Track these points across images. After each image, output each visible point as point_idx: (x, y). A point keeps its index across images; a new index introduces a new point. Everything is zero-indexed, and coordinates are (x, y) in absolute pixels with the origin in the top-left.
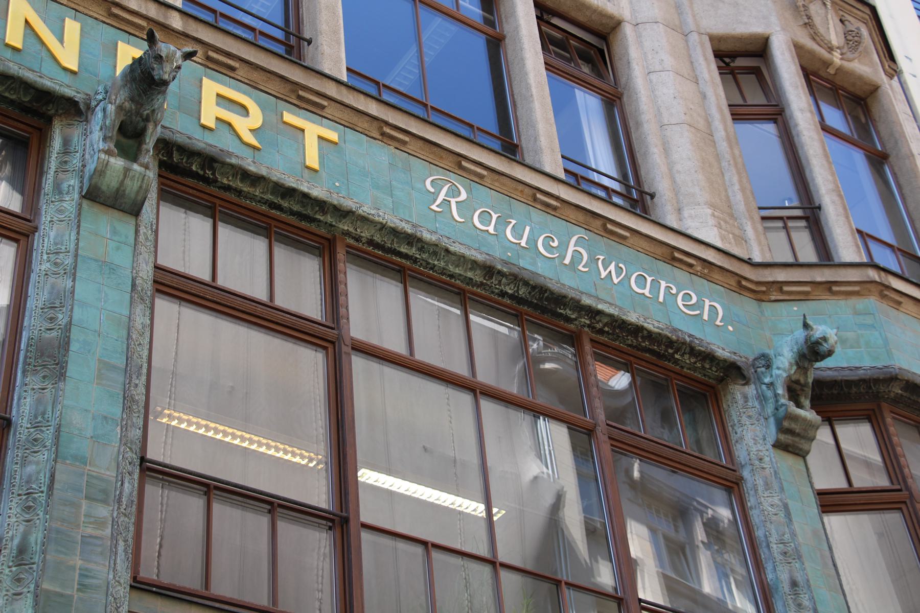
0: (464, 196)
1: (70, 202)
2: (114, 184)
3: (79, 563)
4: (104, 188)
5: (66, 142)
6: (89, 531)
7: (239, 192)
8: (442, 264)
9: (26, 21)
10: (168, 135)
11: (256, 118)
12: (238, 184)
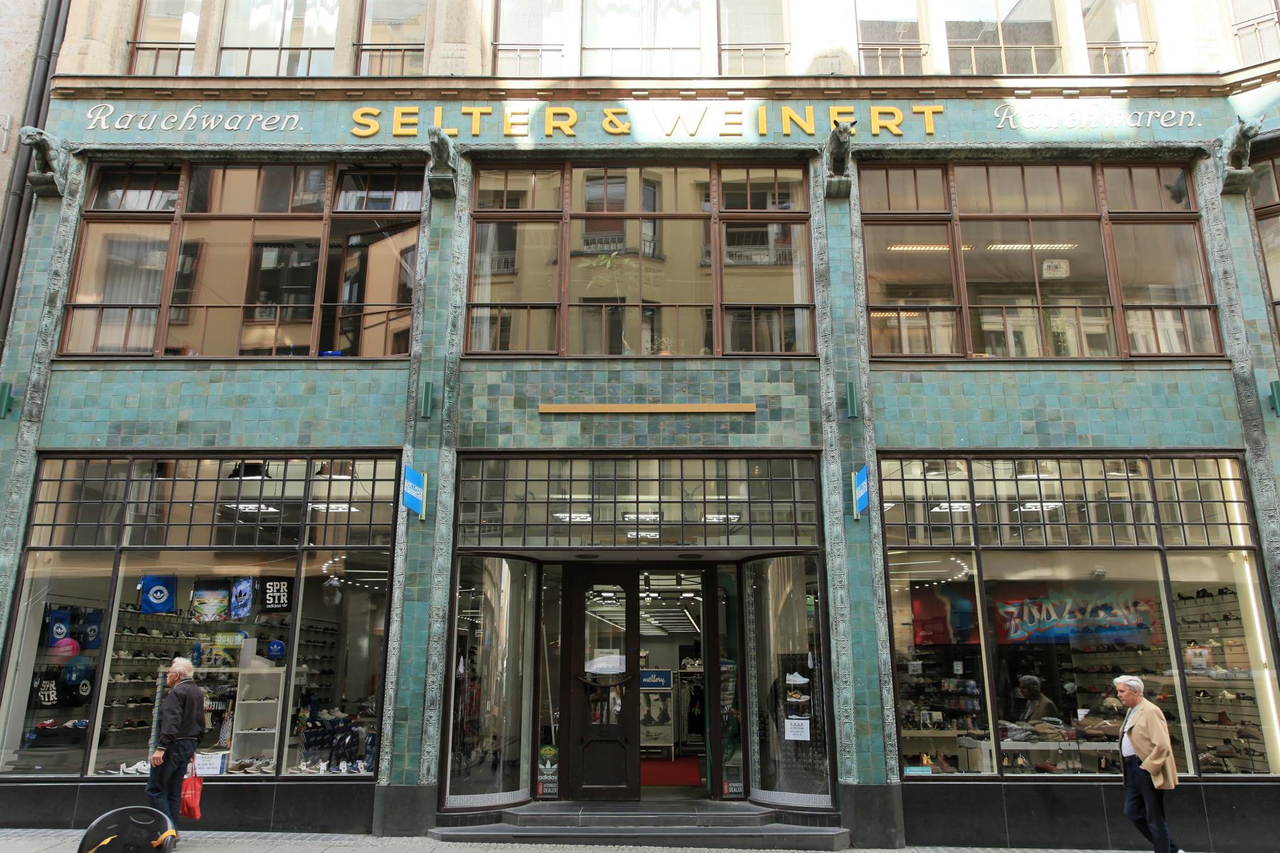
1: (821, 203)
2: (836, 189)
3: (847, 359)
4: (832, 192)
5: (815, 172)
6: (849, 346)
7: (897, 159)
8: (1007, 156)
9: (791, 118)
10: (857, 148)
12: (895, 156)
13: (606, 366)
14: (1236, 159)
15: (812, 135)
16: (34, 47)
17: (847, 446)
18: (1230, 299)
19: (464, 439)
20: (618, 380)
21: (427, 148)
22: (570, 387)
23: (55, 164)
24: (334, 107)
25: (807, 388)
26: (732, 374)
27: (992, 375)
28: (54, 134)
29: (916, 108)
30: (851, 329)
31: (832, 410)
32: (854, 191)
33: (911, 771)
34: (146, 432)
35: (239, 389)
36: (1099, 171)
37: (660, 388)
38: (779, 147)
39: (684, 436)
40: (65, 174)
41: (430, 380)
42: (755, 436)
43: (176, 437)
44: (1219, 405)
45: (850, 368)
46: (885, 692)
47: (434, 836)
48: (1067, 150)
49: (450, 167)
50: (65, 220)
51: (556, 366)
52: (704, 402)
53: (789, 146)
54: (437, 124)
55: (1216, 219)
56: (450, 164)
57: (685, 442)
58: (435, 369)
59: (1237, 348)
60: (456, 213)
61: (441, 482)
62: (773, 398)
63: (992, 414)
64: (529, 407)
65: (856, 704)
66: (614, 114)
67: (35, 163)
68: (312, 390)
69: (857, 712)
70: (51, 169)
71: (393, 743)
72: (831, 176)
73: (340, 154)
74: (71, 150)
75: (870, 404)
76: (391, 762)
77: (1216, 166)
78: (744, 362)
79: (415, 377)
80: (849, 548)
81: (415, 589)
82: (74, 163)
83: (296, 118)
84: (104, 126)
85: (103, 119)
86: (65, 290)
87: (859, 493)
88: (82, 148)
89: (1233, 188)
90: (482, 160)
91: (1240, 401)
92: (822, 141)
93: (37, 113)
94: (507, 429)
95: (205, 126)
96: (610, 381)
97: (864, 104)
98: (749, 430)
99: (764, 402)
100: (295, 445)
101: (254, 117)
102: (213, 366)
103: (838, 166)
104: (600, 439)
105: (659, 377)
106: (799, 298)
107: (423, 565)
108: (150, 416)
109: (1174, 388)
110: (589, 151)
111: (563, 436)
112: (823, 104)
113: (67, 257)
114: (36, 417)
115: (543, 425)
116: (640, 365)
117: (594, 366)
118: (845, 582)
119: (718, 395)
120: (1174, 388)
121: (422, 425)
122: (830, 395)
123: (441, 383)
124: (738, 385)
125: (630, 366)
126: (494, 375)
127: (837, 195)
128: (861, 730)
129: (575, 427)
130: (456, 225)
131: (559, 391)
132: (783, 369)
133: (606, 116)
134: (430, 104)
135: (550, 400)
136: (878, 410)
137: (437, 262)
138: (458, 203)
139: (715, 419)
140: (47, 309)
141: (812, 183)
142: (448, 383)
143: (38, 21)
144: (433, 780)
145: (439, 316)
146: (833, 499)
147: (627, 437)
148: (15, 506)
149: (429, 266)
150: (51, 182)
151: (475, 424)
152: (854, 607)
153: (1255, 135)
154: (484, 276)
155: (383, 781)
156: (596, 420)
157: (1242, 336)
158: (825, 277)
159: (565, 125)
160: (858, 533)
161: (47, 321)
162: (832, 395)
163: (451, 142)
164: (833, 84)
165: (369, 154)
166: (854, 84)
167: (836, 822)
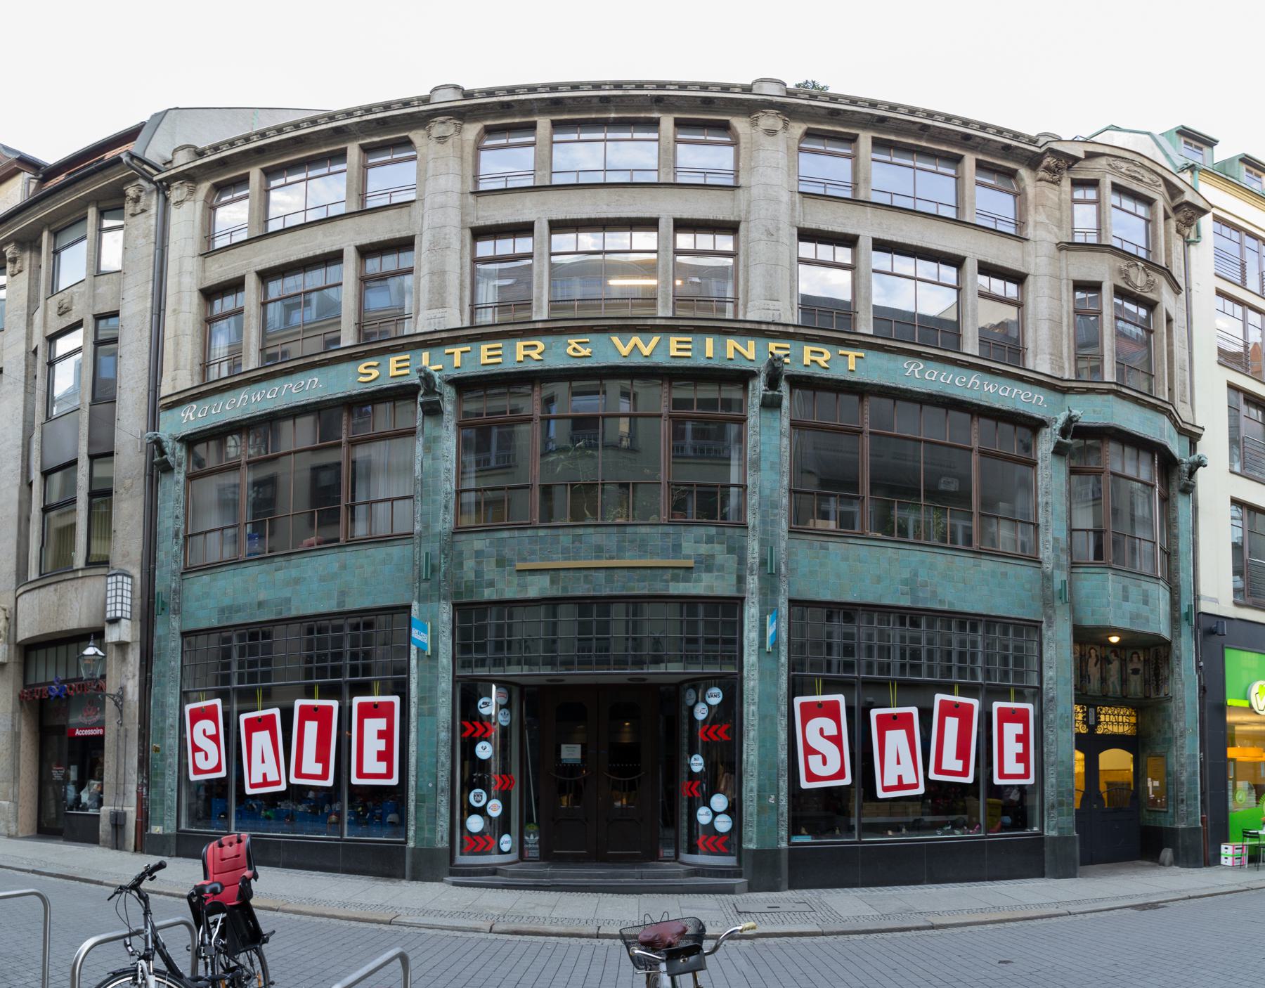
1: (757, 409)
22: (541, 549)
25: (739, 551)
26: (675, 536)
30: (775, 505)
32: (786, 403)
38: (723, 367)
39: (632, 584)
42: (691, 584)
45: (772, 535)
49: (436, 392)
52: (651, 558)
53: (732, 367)
56: (436, 390)
57: (633, 589)
58: (433, 542)
60: (444, 425)
62: (708, 556)
64: (508, 566)
66: (577, 343)
72: (766, 390)
78: (686, 527)
79: (418, 549)
92: (761, 366)
94: (491, 584)
96: (573, 543)
103: (773, 382)
104: (564, 589)
106: (734, 480)
115: (519, 579)
122: (754, 556)
123: (438, 552)
124: (680, 546)
126: (479, 543)
127: (771, 404)
131: (533, 553)
132: (717, 533)
133: (570, 345)
137: (430, 461)
138: (445, 417)
141: (750, 395)
142: (443, 551)
145: (434, 501)
149: (424, 465)
151: (466, 582)
154: (470, 472)
156: (562, 574)
158: (756, 465)
159: (534, 354)
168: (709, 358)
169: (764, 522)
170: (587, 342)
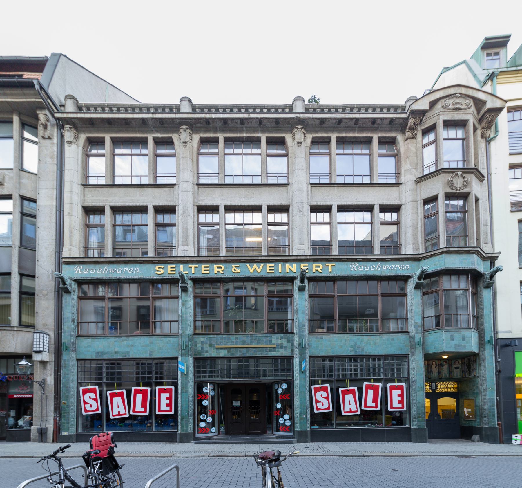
0: (357, 265)
1: (297, 291)
10: (308, 276)
11: (322, 267)
13: (235, 336)
14: (419, 278)
15: (295, 272)
16: (55, 249)
17: (301, 355)
18: (412, 317)
19: (195, 354)
20: (238, 339)
21: (178, 277)
23: (67, 283)
24: (149, 266)
25: (292, 341)
27: (343, 337)
28: (66, 275)
29: (327, 265)
30: (304, 325)
31: (297, 346)
32: (307, 288)
33: (313, 428)
34: (106, 354)
35: (130, 343)
36: (379, 282)
37: (249, 341)
40: (71, 286)
41: (185, 340)
43: (115, 355)
44: (404, 344)
46: (308, 411)
47: (193, 443)
48: (371, 276)
49: (186, 283)
50: (73, 299)
51: (220, 336)
53: (288, 276)
54: (181, 270)
55: (411, 295)
59: (412, 329)
61: (189, 365)
63: (342, 347)
65: (300, 414)
67: (61, 283)
68: (152, 343)
69: (300, 415)
70: (66, 284)
71: (181, 424)
73: (153, 279)
74: (71, 279)
75: (308, 344)
76: (181, 428)
77: (414, 280)
80: (300, 379)
81: (184, 390)
82: (73, 283)
83: (138, 269)
84: (80, 272)
85: (79, 270)
86: (77, 318)
87: (303, 366)
88: (74, 278)
89: (417, 287)
90: (196, 281)
91: (410, 343)
92: (298, 275)
93: (59, 269)
94: (207, 352)
95: (111, 272)
97: (311, 263)
98: (274, 351)
99: (278, 345)
100: (148, 357)
101: (125, 269)
102: (122, 337)
103: (302, 281)
104: (233, 354)
105: (249, 338)
107: (186, 385)
108: (107, 350)
109: (393, 340)
110: (228, 278)
111: (223, 353)
112: (299, 263)
113: (76, 309)
114: (75, 351)
116: (244, 335)
117: (231, 336)
118: (299, 387)
119: (266, 343)
120: (393, 340)
121: (183, 351)
124: (271, 340)
125: (241, 336)
126: (202, 338)
127: (302, 289)
128: (301, 419)
129: (226, 351)
130: (189, 299)
131: (221, 342)
134: (179, 264)
135: (219, 345)
136: (310, 346)
137: (184, 309)
139: (265, 349)
140: (72, 323)
143: (54, 241)
144: (192, 431)
145: (186, 323)
146: (296, 368)
147: (240, 354)
148: (73, 372)
150: (67, 288)
152: (301, 392)
153: (426, 272)
155: (179, 432)
156: (232, 349)
157: (413, 326)
158: (297, 312)
160: (303, 376)
161: (73, 326)
162: (297, 342)
163: (185, 275)
164: (302, 258)
165: (161, 279)
166: (308, 258)
167: (293, 438)
168: (280, 273)
169: (300, 331)
170: (239, 267)
